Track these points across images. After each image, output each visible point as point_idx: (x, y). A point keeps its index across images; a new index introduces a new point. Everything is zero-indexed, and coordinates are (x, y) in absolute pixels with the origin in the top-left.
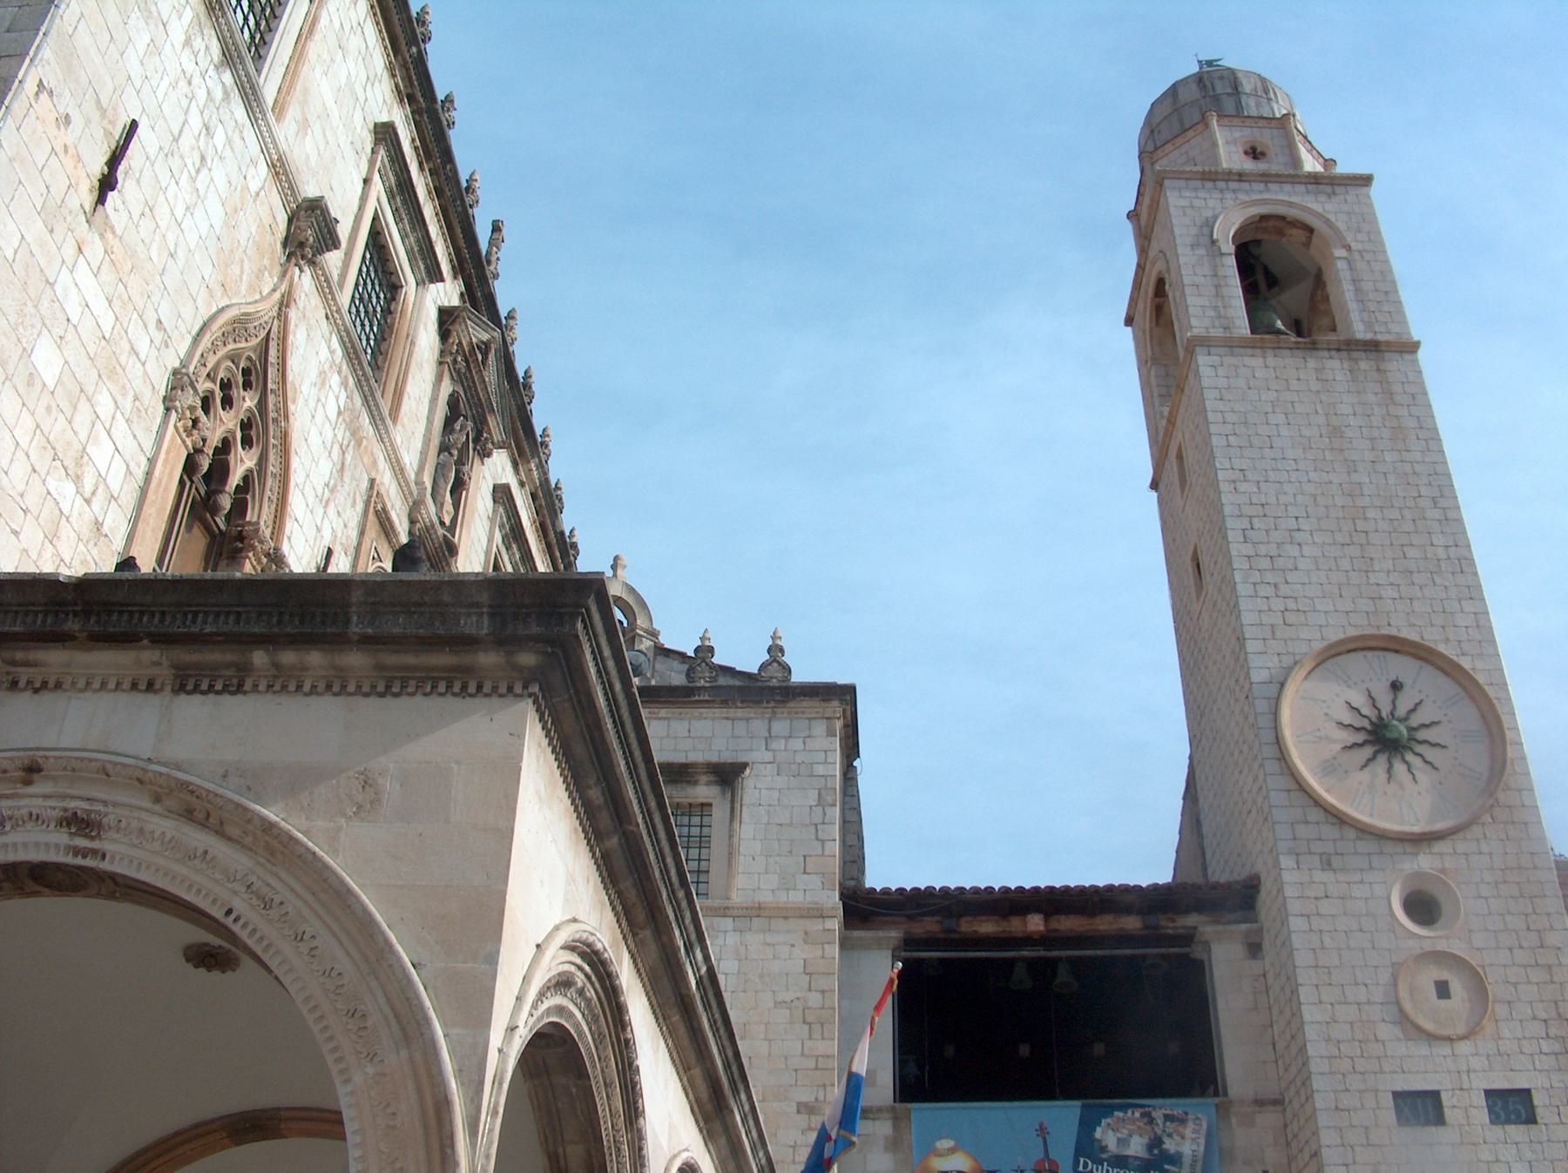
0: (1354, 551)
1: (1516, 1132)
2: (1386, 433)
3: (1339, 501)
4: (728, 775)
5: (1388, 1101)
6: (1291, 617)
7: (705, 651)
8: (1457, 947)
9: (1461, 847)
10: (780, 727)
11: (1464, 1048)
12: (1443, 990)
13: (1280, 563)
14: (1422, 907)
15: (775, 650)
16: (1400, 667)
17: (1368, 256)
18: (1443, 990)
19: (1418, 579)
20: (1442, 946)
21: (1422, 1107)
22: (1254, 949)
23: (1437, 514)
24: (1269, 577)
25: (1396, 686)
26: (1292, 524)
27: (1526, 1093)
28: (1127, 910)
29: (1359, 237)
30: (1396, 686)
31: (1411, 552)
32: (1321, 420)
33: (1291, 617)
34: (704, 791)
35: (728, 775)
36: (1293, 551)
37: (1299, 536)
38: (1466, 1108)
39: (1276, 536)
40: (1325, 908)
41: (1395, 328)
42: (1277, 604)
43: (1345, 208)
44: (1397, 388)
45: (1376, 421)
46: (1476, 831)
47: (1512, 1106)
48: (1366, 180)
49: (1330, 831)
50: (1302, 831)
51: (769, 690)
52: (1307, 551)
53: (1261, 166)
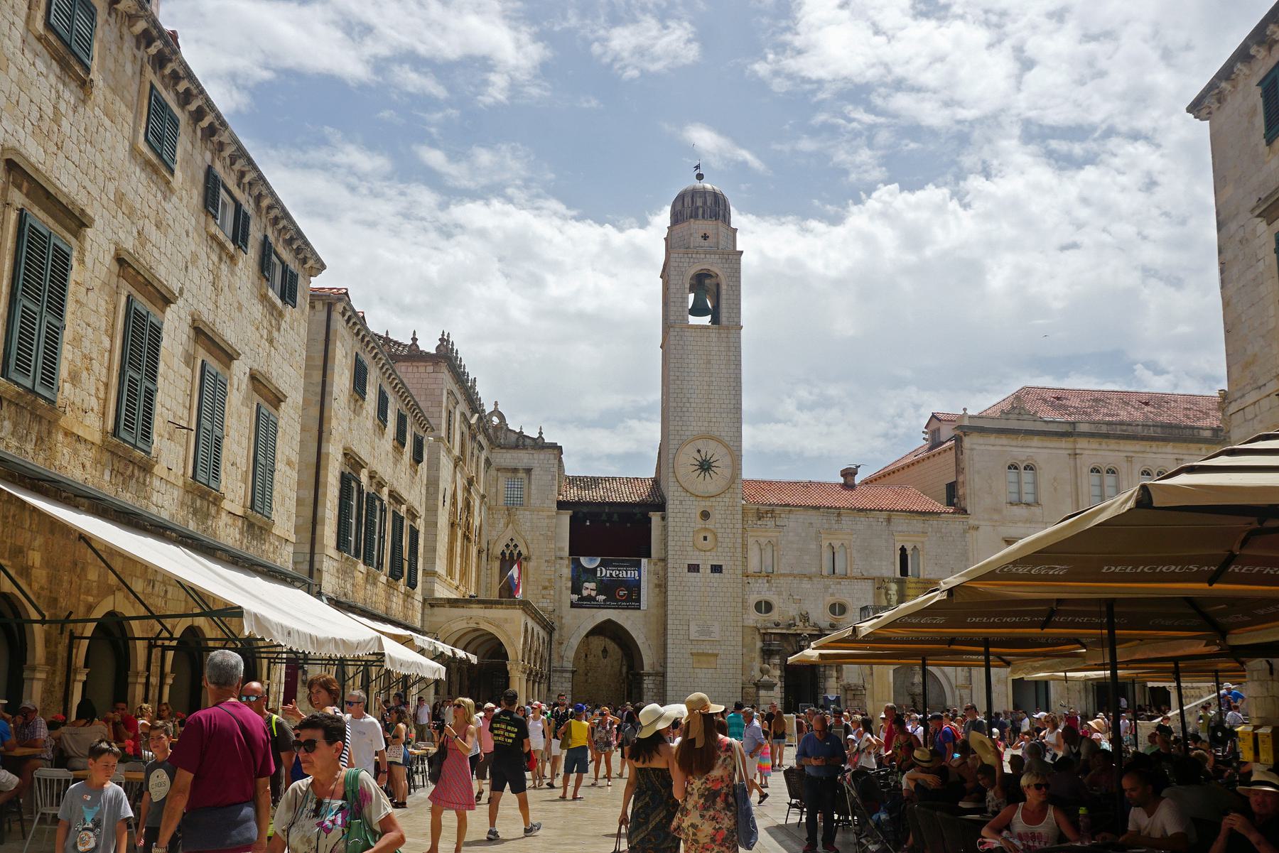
1: (717, 575)
4: (528, 471)
7: (521, 432)
10: (542, 457)
12: (705, 538)
14: (705, 515)
15: (541, 433)
18: (705, 538)
21: (694, 568)
22: (663, 518)
27: (721, 566)
34: (521, 475)
35: (528, 471)
38: (705, 569)
47: (717, 569)
48: (741, 252)
51: (539, 444)
53: (706, 243)
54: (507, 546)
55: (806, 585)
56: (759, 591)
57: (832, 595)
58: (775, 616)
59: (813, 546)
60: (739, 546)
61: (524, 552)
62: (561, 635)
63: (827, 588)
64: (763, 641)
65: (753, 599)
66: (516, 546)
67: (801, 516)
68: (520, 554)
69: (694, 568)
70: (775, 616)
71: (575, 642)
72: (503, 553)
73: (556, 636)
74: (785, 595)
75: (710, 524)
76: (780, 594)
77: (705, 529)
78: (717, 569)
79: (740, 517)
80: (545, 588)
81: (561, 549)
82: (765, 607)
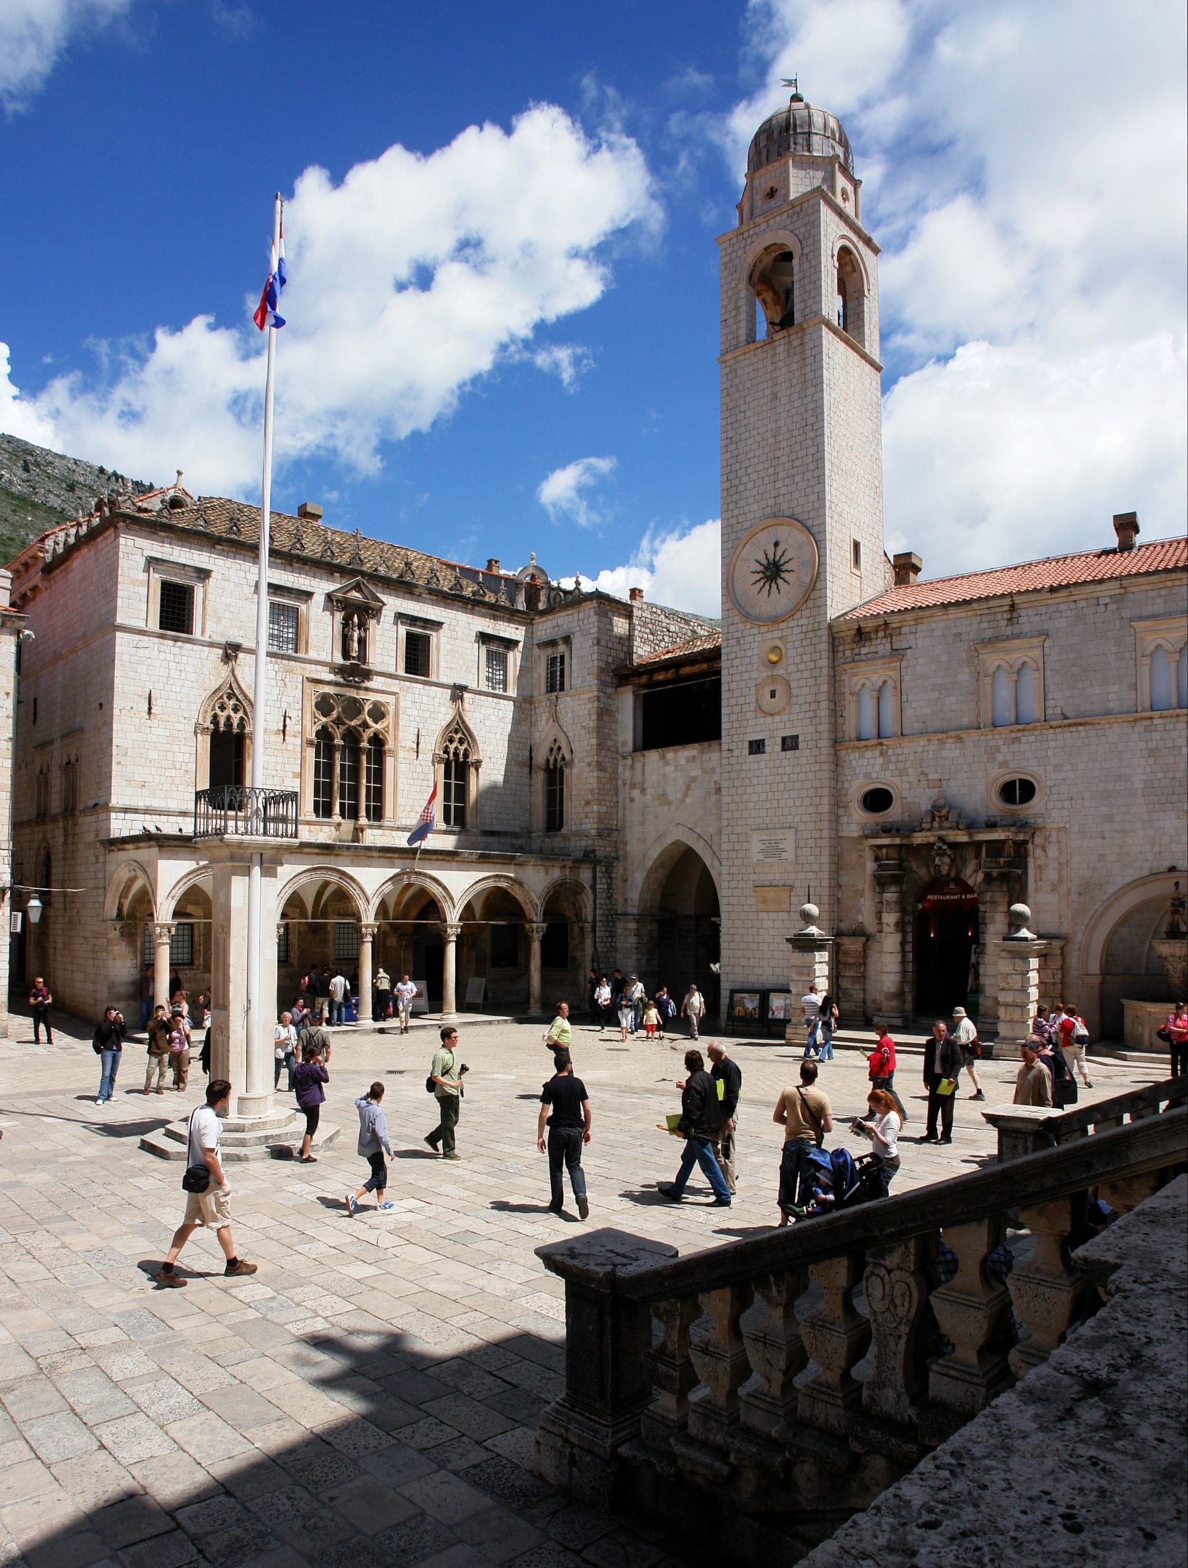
0: (771, 471)
2: (798, 388)
3: (770, 441)
5: (747, 745)
6: (741, 519)
8: (781, 672)
9: (792, 623)
10: (581, 616)
11: (777, 718)
13: (742, 488)
16: (782, 532)
17: (811, 256)
19: (798, 478)
20: (776, 672)
21: (757, 747)
23: (811, 434)
24: (735, 498)
25: (776, 544)
26: (746, 463)
28: (701, 662)
29: (810, 241)
30: (776, 544)
31: (798, 463)
32: (768, 392)
33: (741, 519)
35: (567, 640)
36: (745, 479)
37: (750, 470)
38: (773, 746)
39: (741, 473)
40: (736, 662)
41: (814, 308)
42: (736, 513)
43: (806, 220)
44: (808, 353)
45: (794, 381)
46: (798, 615)
47: (790, 744)
49: (741, 627)
50: (732, 629)
52: (754, 476)
53: (772, 203)
54: (551, 750)
55: (952, 752)
56: (867, 770)
57: (1003, 764)
58: (895, 813)
59: (964, 677)
60: (823, 697)
61: (568, 757)
62: (625, 869)
63: (992, 752)
64: (877, 859)
65: (857, 788)
66: (559, 748)
67: (938, 624)
68: (563, 758)
69: (757, 747)
70: (895, 813)
71: (638, 878)
72: (548, 761)
73: (618, 871)
74: (912, 775)
75: (780, 671)
76: (903, 772)
77: (773, 678)
78: (790, 744)
79: (824, 646)
80: (588, 803)
81: (624, 744)
82: (877, 800)
